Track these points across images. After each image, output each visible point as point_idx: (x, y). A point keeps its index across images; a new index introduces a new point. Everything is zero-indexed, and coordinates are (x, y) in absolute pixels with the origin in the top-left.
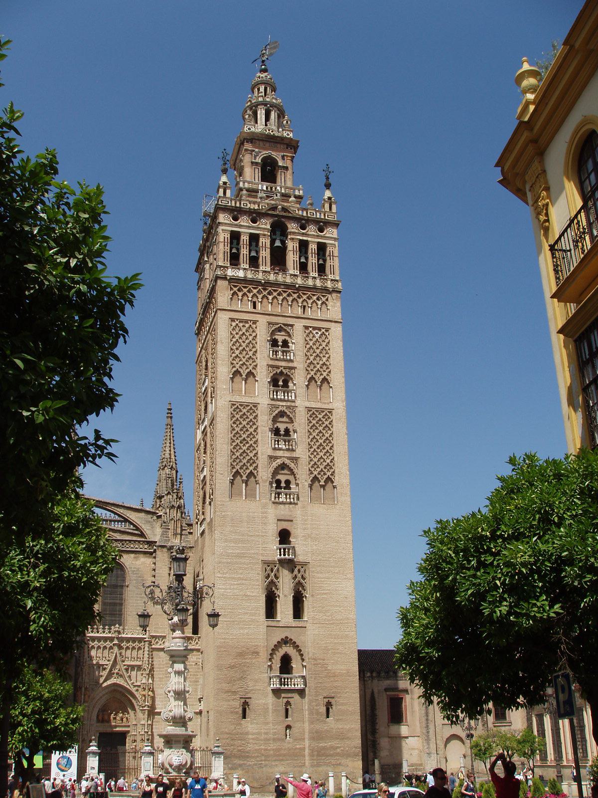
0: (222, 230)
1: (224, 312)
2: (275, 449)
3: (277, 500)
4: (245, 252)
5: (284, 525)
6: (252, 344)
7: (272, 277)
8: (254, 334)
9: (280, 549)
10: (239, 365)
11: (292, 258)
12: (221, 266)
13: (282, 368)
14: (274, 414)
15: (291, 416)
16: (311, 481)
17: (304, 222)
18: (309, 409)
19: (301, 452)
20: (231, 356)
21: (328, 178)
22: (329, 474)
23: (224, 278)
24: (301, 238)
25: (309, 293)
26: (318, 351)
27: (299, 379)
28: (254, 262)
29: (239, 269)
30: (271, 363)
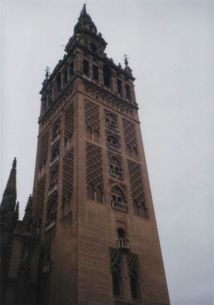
0: (79, 56)
1: (81, 94)
2: (112, 176)
3: (116, 207)
4: (91, 71)
5: (122, 226)
6: (97, 116)
7: (105, 88)
8: (97, 112)
9: (121, 241)
10: (90, 124)
11: (115, 85)
12: (79, 72)
13: (113, 134)
14: (110, 157)
15: (119, 161)
16: (133, 201)
17: (119, 71)
18: (129, 161)
19: (126, 182)
20: (86, 118)
21: (126, 60)
22: (142, 200)
23: (82, 78)
24: (118, 78)
25: (124, 104)
26: (130, 133)
27: (122, 142)
28: (96, 77)
29: (89, 77)
30: (107, 129)
